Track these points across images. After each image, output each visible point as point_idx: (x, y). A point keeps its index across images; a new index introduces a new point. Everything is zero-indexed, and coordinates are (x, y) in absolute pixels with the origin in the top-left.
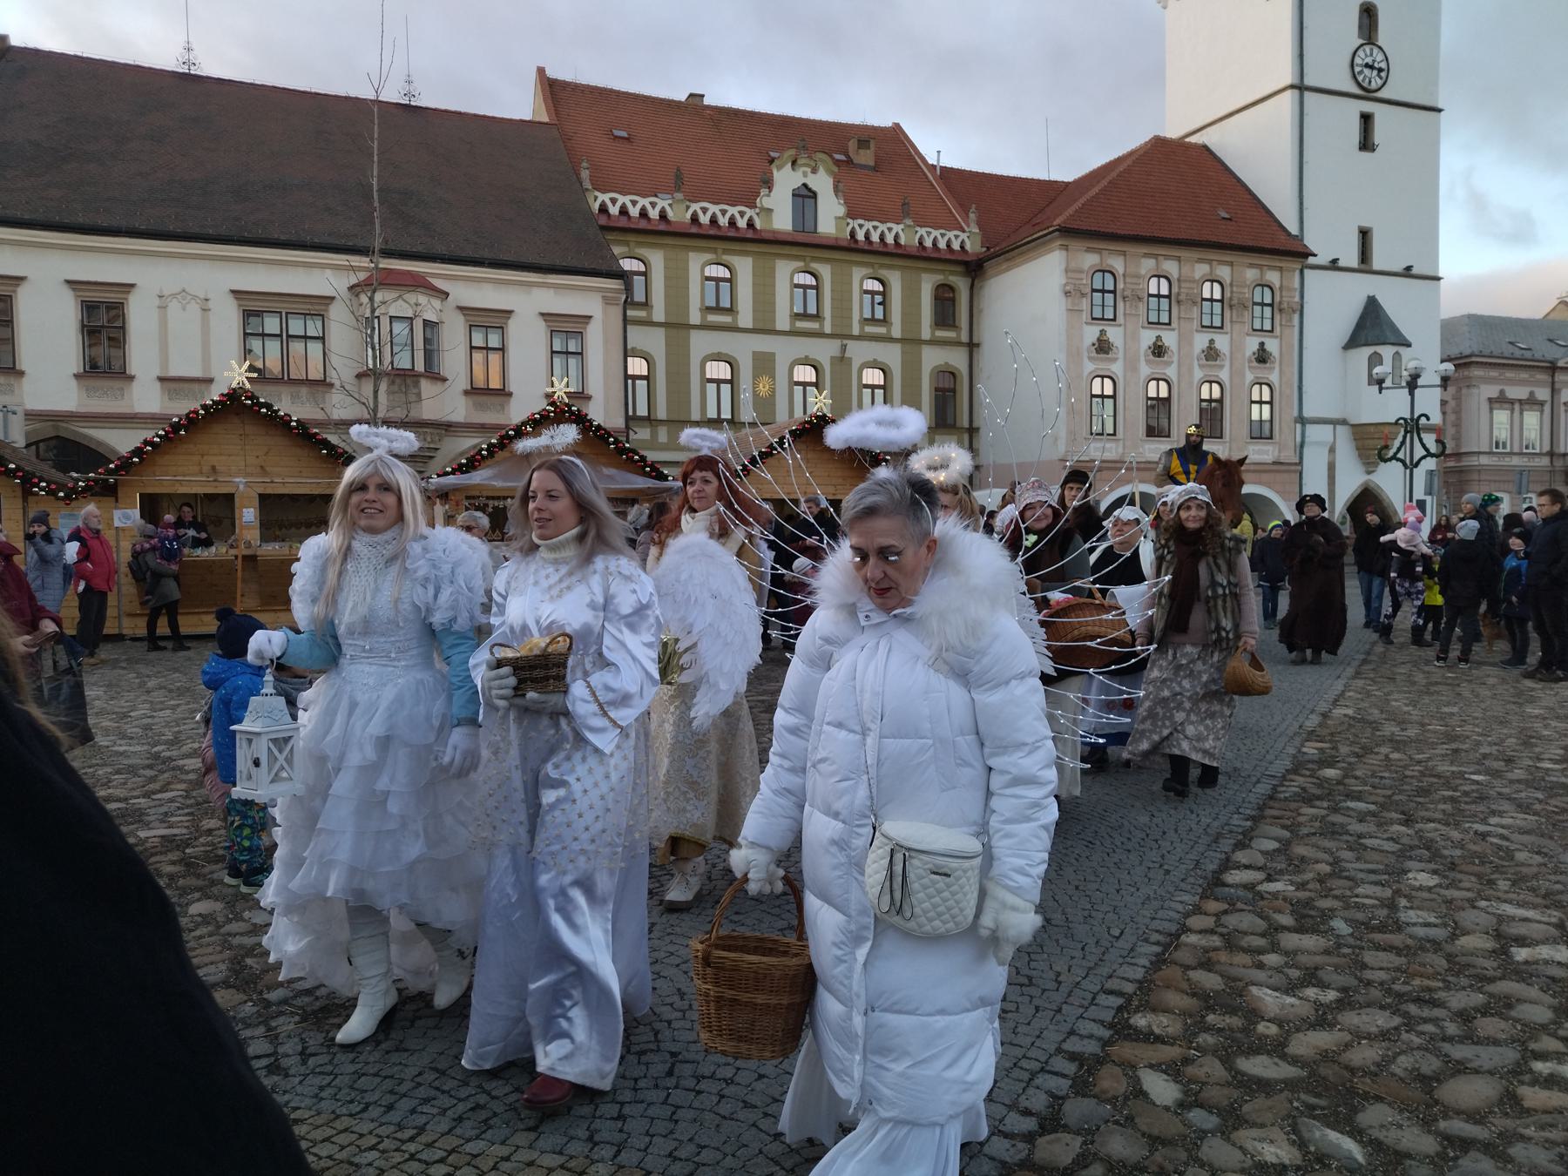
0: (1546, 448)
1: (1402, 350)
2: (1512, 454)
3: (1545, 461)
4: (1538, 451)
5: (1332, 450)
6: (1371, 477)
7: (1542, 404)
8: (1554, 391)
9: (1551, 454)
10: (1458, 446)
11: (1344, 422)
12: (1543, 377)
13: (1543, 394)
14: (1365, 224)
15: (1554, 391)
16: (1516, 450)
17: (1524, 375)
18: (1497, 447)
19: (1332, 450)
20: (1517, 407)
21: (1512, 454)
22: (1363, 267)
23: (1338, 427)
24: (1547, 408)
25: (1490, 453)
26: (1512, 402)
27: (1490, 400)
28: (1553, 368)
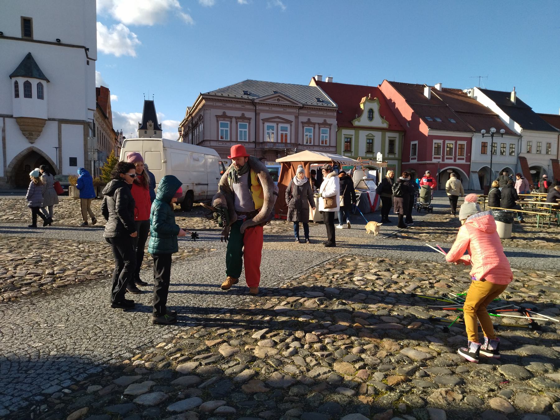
0: (253, 139)
1: (44, 83)
2: (330, 146)
3: (253, 146)
4: (247, 141)
5: (4, 131)
6: (29, 145)
7: (249, 119)
8: (257, 114)
9: (255, 142)
10: (204, 137)
11: (11, 117)
12: (252, 107)
13: (250, 115)
14: (27, 15)
15: (257, 114)
16: (317, 144)
17: (238, 106)
18: (322, 143)
19: (4, 131)
20: (317, 126)
21: (330, 146)
22: (25, 38)
23: (6, 119)
24: (253, 122)
25: (218, 141)
26: (231, 118)
27: (217, 117)
28: (253, 103)
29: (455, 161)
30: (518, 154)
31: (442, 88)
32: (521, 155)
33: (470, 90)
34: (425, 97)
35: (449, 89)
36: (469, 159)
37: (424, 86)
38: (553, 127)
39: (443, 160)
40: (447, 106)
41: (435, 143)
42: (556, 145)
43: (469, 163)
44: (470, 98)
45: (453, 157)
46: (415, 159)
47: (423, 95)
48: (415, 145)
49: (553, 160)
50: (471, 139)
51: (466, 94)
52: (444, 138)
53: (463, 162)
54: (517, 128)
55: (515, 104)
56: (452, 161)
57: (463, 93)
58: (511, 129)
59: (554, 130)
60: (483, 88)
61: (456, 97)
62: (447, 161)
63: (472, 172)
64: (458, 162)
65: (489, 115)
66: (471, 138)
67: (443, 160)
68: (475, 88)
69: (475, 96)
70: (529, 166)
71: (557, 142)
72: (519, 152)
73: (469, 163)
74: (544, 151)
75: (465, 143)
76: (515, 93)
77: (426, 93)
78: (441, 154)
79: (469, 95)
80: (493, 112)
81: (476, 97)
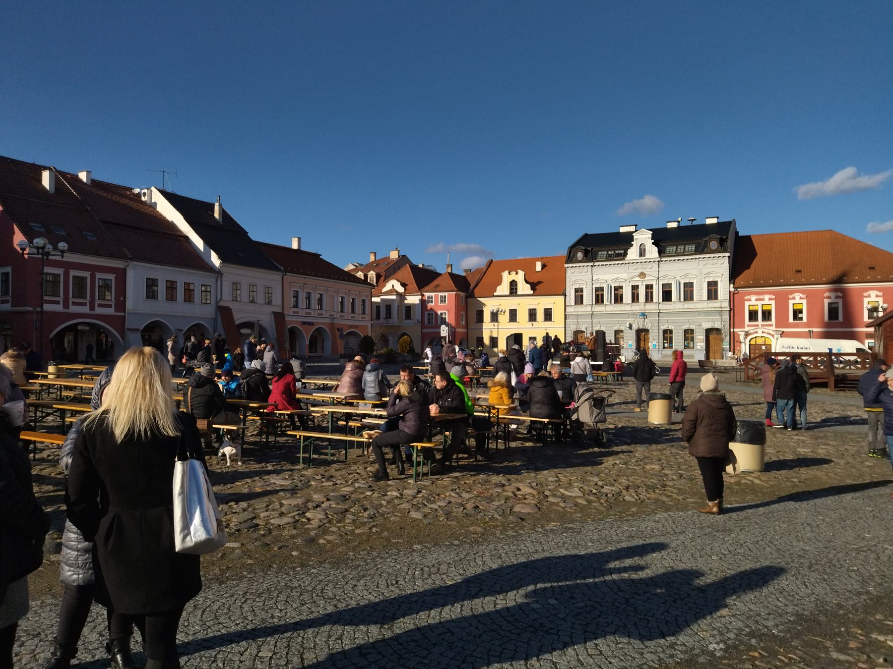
29: (92, 308)
30: (217, 302)
31: (93, 181)
32: (222, 304)
33: (146, 191)
34: (44, 188)
35: (108, 184)
36: (121, 305)
37: (41, 168)
38: (278, 265)
39: (66, 306)
40: (87, 211)
41: (99, 279)
42: (280, 291)
43: (122, 314)
44: (144, 203)
45: (88, 302)
46: (7, 302)
47: (41, 183)
48: (7, 274)
49: (275, 314)
50: (124, 271)
51: (139, 195)
52: (94, 269)
53: (111, 311)
54: (215, 260)
55: (221, 223)
56: (86, 310)
57: (134, 194)
58: (206, 260)
59: (276, 269)
60: (169, 190)
61: (116, 198)
62: (73, 309)
63: (129, 329)
64: (99, 311)
65: (170, 234)
66: (125, 269)
67: (66, 306)
68: (153, 189)
69: (153, 201)
70: (237, 323)
71: (280, 287)
72: (219, 299)
73: (122, 314)
74: (260, 299)
75: (112, 277)
76: (220, 205)
77: (46, 179)
78: (62, 295)
79: (143, 199)
80: (180, 231)
81: (155, 203)
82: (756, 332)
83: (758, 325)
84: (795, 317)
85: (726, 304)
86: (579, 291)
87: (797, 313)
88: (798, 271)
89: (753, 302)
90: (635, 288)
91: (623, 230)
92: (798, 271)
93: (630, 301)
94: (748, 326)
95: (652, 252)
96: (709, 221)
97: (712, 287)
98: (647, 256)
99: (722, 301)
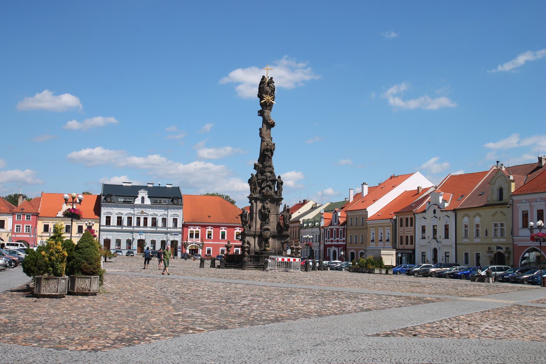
82: (193, 243)
83: (193, 240)
84: (208, 237)
85: (181, 230)
86: (108, 219)
87: (209, 235)
88: (209, 217)
89: (192, 229)
90: (139, 219)
91: (124, 184)
92: (209, 217)
93: (135, 225)
94: (189, 240)
95: (148, 202)
96: (168, 186)
97: (175, 221)
98: (145, 203)
99: (179, 228)
